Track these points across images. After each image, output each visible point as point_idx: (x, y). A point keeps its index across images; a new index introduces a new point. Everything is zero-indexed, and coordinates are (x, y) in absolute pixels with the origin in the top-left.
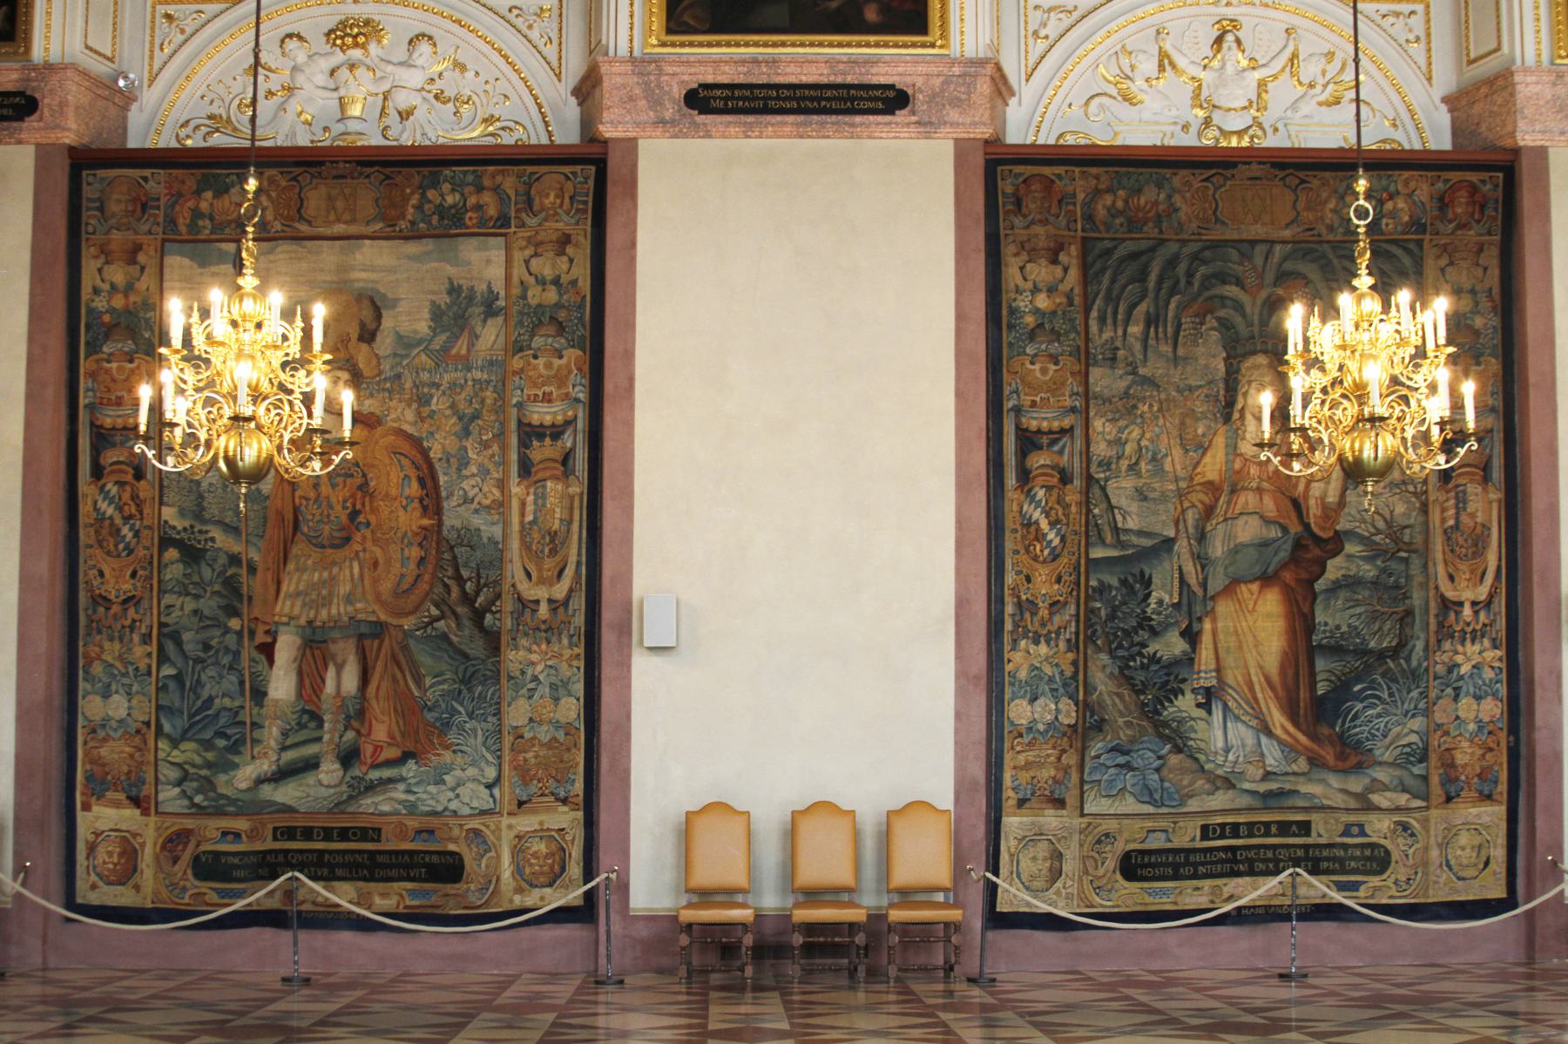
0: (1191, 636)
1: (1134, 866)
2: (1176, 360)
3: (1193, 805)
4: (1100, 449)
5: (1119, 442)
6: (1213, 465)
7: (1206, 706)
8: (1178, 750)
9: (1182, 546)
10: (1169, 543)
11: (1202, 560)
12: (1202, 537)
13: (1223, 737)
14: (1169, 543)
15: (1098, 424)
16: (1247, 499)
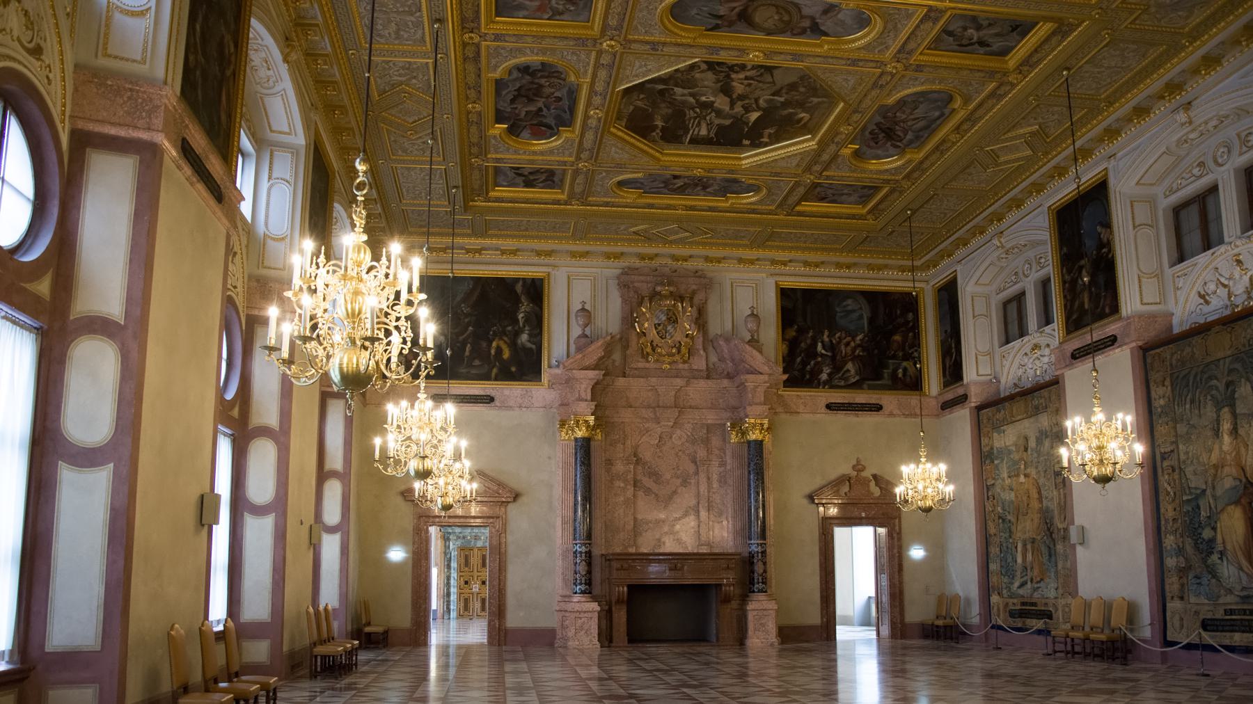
0: (1214, 529)
1: (1206, 625)
2: (1200, 416)
3: (1221, 601)
4: (1183, 457)
5: (1187, 453)
6: (1215, 457)
7: (1221, 559)
8: (1214, 577)
9: (1208, 492)
10: (1204, 491)
11: (1214, 496)
12: (1214, 488)
13: (1227, 571)
14: (1204, 491)
15: (1181, 446)
16: (1227, 470)
